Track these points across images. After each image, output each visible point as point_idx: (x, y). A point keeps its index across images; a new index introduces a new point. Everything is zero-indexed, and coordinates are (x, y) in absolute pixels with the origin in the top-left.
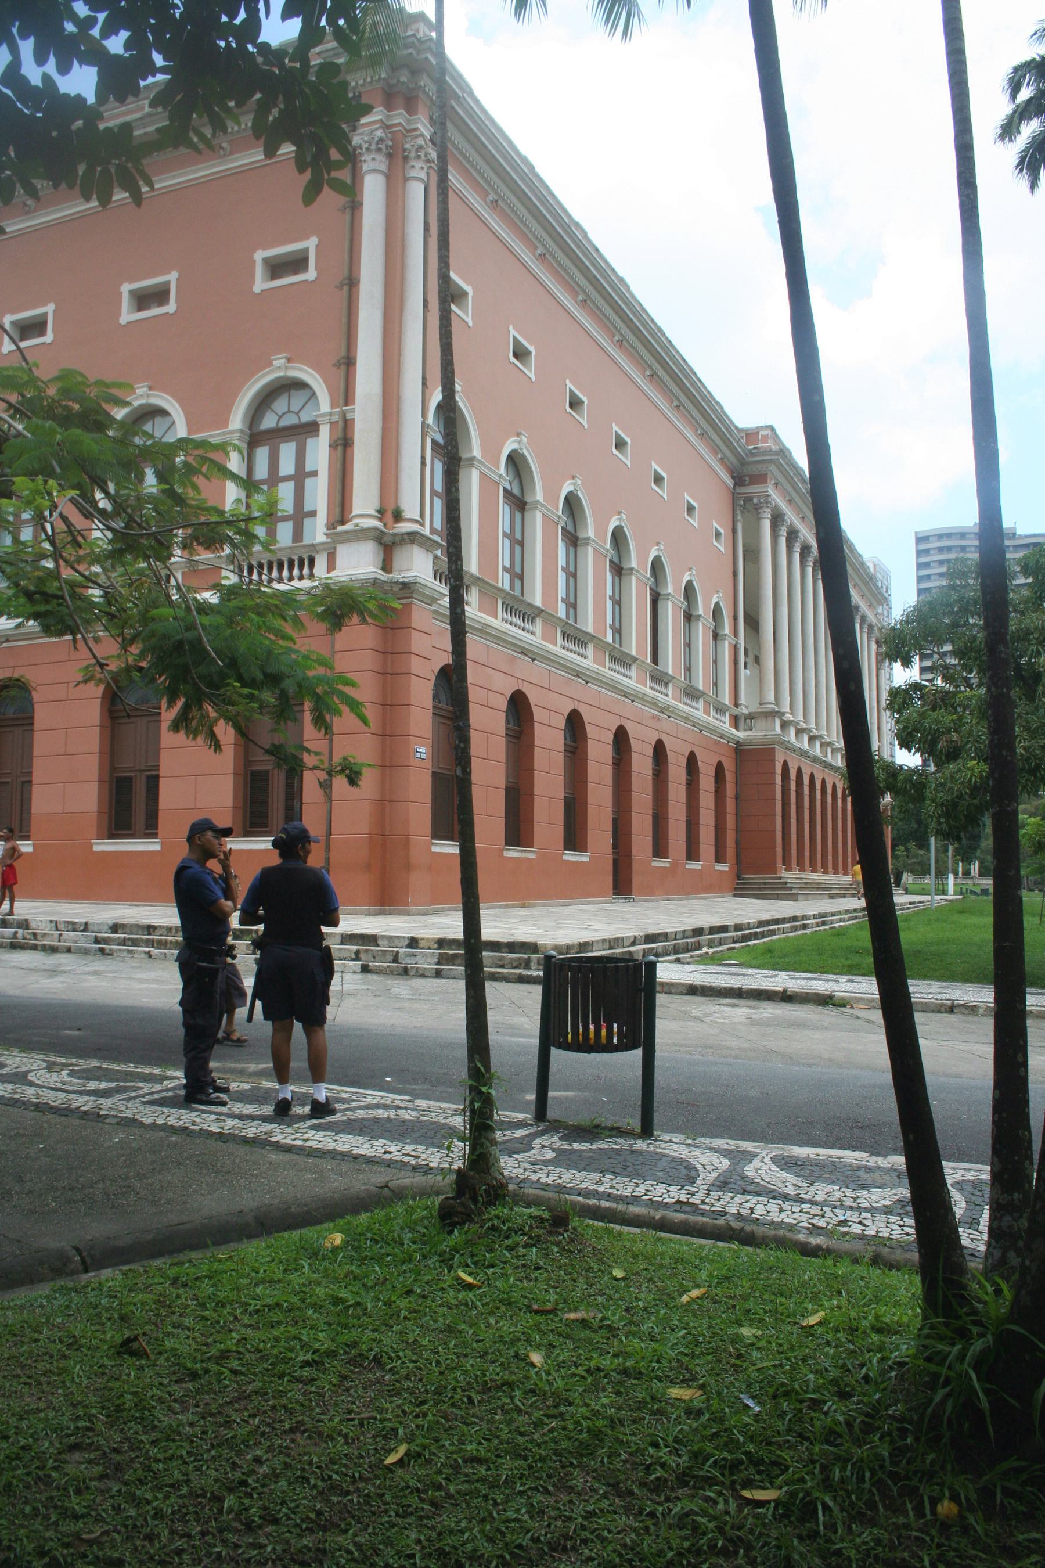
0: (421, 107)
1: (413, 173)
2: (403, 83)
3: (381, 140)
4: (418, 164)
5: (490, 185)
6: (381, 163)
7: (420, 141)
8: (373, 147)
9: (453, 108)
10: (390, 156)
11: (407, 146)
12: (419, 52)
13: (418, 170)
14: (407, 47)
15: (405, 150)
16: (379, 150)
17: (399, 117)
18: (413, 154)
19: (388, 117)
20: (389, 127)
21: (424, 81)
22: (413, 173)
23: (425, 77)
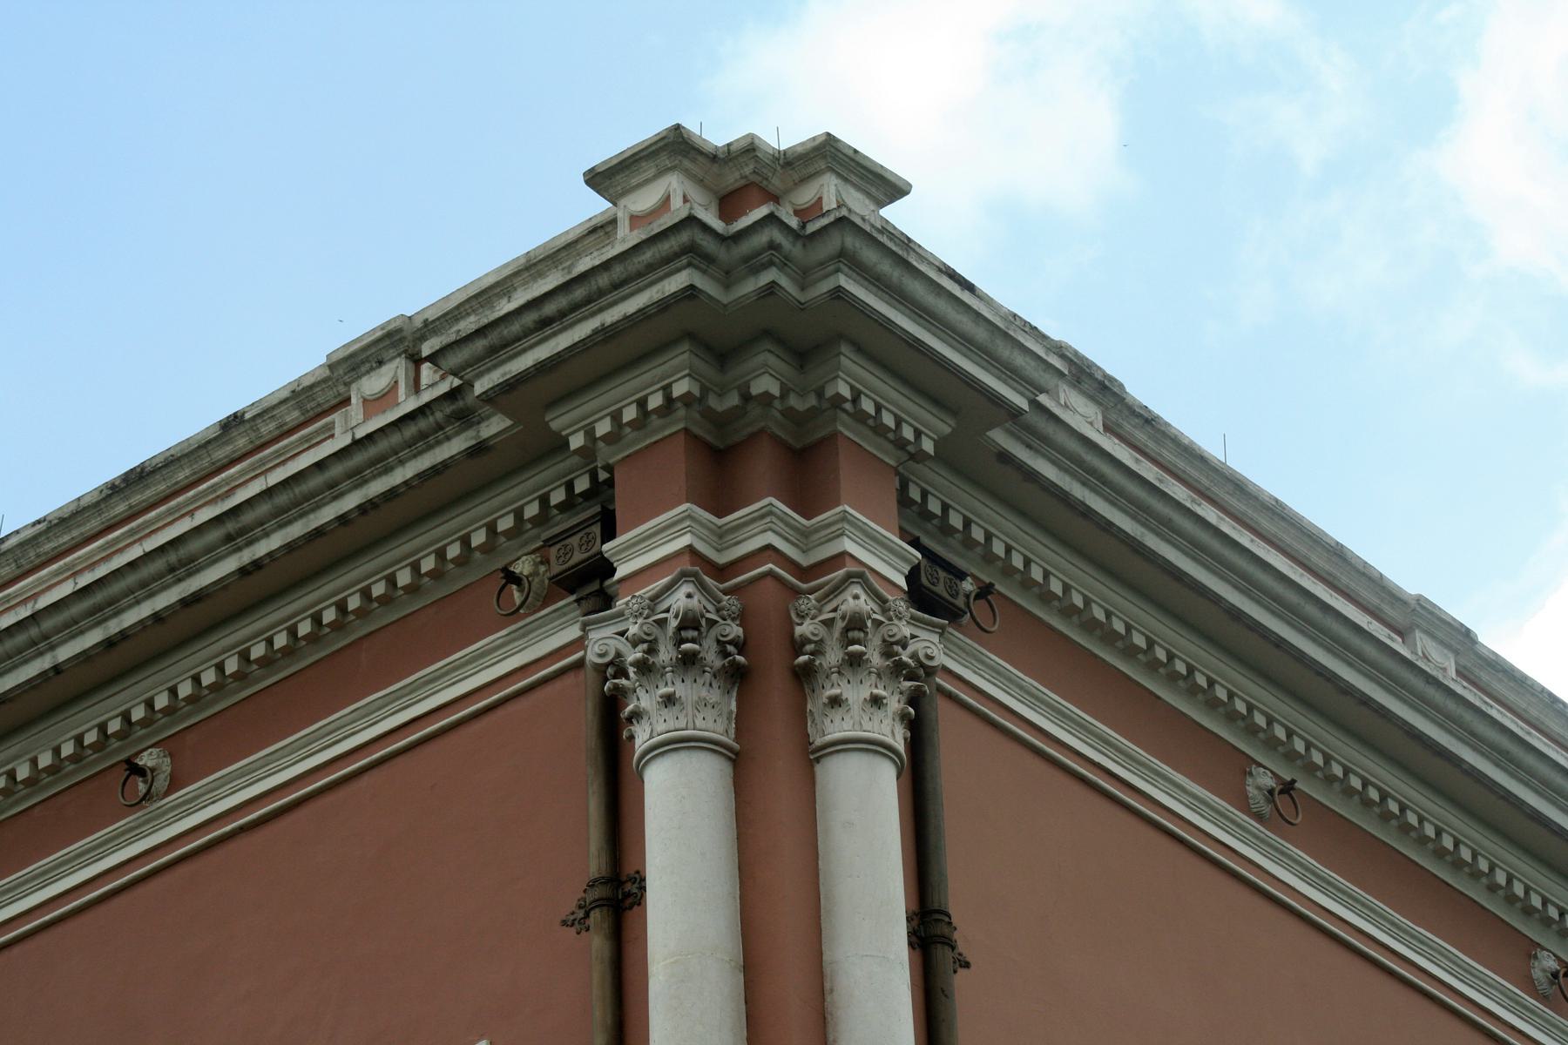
0: (848, 474)
1: (838, 727)
2: (766, 398)
3: (690, 623)
4: (856, 692)
5: (1252, 731)
6: (705, 708)
7: (856, 601)
8: (666, 654)
9: (1005, 457)
10: (737, 677)
11: (805, 629)
12: (805, 277)
13: (863, 712)
14: (754, 264)
15: (797, 646)
16: (688, 662)
17: (764, 527)
18: (833, 656)
19: (722, 537)
20: (721, 572)
21: (849, 376)
22: (838, 727)
23: (848, 361)
